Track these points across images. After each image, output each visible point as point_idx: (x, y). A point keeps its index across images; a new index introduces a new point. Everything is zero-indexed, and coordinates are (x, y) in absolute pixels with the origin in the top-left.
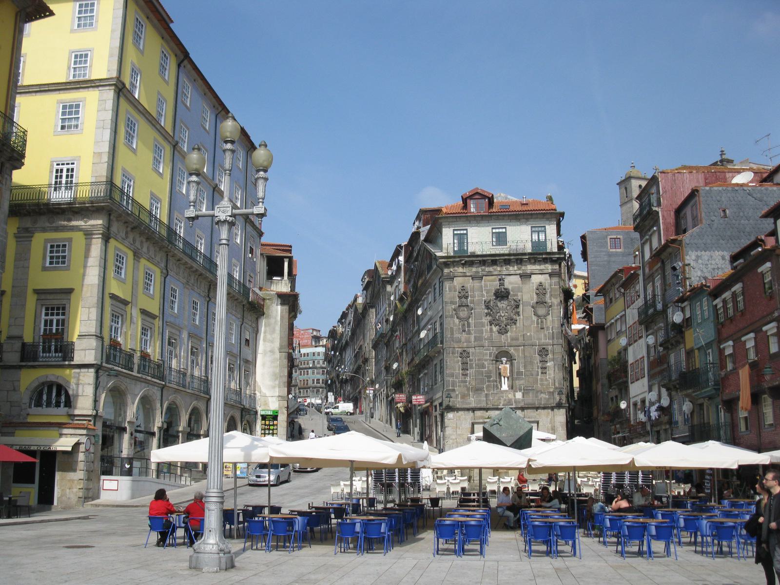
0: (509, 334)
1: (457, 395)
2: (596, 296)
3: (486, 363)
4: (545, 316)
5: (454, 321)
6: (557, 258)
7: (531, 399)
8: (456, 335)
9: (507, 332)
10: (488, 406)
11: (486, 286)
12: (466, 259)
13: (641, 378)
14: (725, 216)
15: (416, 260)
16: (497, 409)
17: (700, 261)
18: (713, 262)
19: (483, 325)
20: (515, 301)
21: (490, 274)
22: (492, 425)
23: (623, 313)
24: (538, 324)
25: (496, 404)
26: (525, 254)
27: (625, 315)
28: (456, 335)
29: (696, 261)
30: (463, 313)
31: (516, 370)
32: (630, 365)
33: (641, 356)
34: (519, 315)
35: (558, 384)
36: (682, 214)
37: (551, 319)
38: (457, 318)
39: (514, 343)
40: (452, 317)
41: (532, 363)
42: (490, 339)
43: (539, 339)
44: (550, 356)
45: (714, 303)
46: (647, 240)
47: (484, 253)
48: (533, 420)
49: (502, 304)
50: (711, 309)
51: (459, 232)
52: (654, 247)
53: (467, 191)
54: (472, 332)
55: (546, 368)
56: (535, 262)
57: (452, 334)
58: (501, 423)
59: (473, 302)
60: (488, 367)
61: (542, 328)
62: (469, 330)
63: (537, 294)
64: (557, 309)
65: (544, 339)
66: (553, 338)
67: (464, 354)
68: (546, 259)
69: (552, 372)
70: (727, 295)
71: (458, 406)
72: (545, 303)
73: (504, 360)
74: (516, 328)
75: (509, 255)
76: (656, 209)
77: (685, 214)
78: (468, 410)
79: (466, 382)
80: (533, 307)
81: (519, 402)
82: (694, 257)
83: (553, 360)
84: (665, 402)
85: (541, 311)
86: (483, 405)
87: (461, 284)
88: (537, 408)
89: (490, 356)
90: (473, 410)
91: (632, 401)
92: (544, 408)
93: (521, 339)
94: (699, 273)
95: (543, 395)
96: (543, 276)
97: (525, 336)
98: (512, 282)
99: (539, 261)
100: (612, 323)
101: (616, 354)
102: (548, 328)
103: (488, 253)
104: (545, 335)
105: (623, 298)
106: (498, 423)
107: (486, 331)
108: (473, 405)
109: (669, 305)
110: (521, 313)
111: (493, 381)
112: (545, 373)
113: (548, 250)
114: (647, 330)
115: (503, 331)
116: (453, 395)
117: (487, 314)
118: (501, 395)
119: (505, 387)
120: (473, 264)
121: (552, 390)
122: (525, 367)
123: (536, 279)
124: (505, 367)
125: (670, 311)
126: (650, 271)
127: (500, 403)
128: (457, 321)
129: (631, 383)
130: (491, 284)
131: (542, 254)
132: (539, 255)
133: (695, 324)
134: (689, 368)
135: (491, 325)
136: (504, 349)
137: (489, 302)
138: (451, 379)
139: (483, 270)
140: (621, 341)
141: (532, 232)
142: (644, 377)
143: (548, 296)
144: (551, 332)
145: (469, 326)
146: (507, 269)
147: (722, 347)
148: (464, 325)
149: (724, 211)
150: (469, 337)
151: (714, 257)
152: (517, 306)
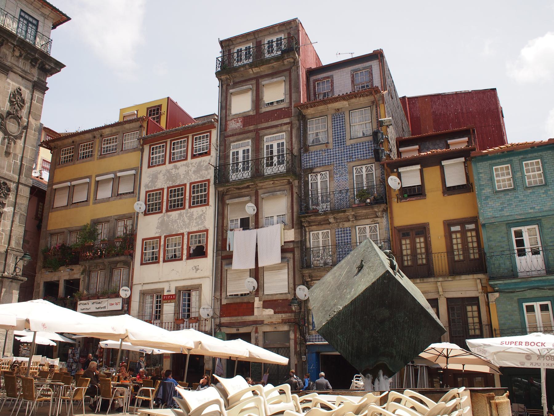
4: (16, 137)
6: (52, 68)
32: (143, 240)
33: (195, 229)
35: (16, 242)
37: (22, 145)
44: (11, 197)
63: (11, 102)
64: (34, 135)
69: (8, 223)
77: (332, 77)
83: (15, 205)
91: (137, 290)
96: (24, 80)
99: (26, 59)
104: (9, 166)
109: (315, 171)
129: (142, 264)
133: (487, 191)
141: (21, 16)
143: (25, 111)
144: (19, 164)
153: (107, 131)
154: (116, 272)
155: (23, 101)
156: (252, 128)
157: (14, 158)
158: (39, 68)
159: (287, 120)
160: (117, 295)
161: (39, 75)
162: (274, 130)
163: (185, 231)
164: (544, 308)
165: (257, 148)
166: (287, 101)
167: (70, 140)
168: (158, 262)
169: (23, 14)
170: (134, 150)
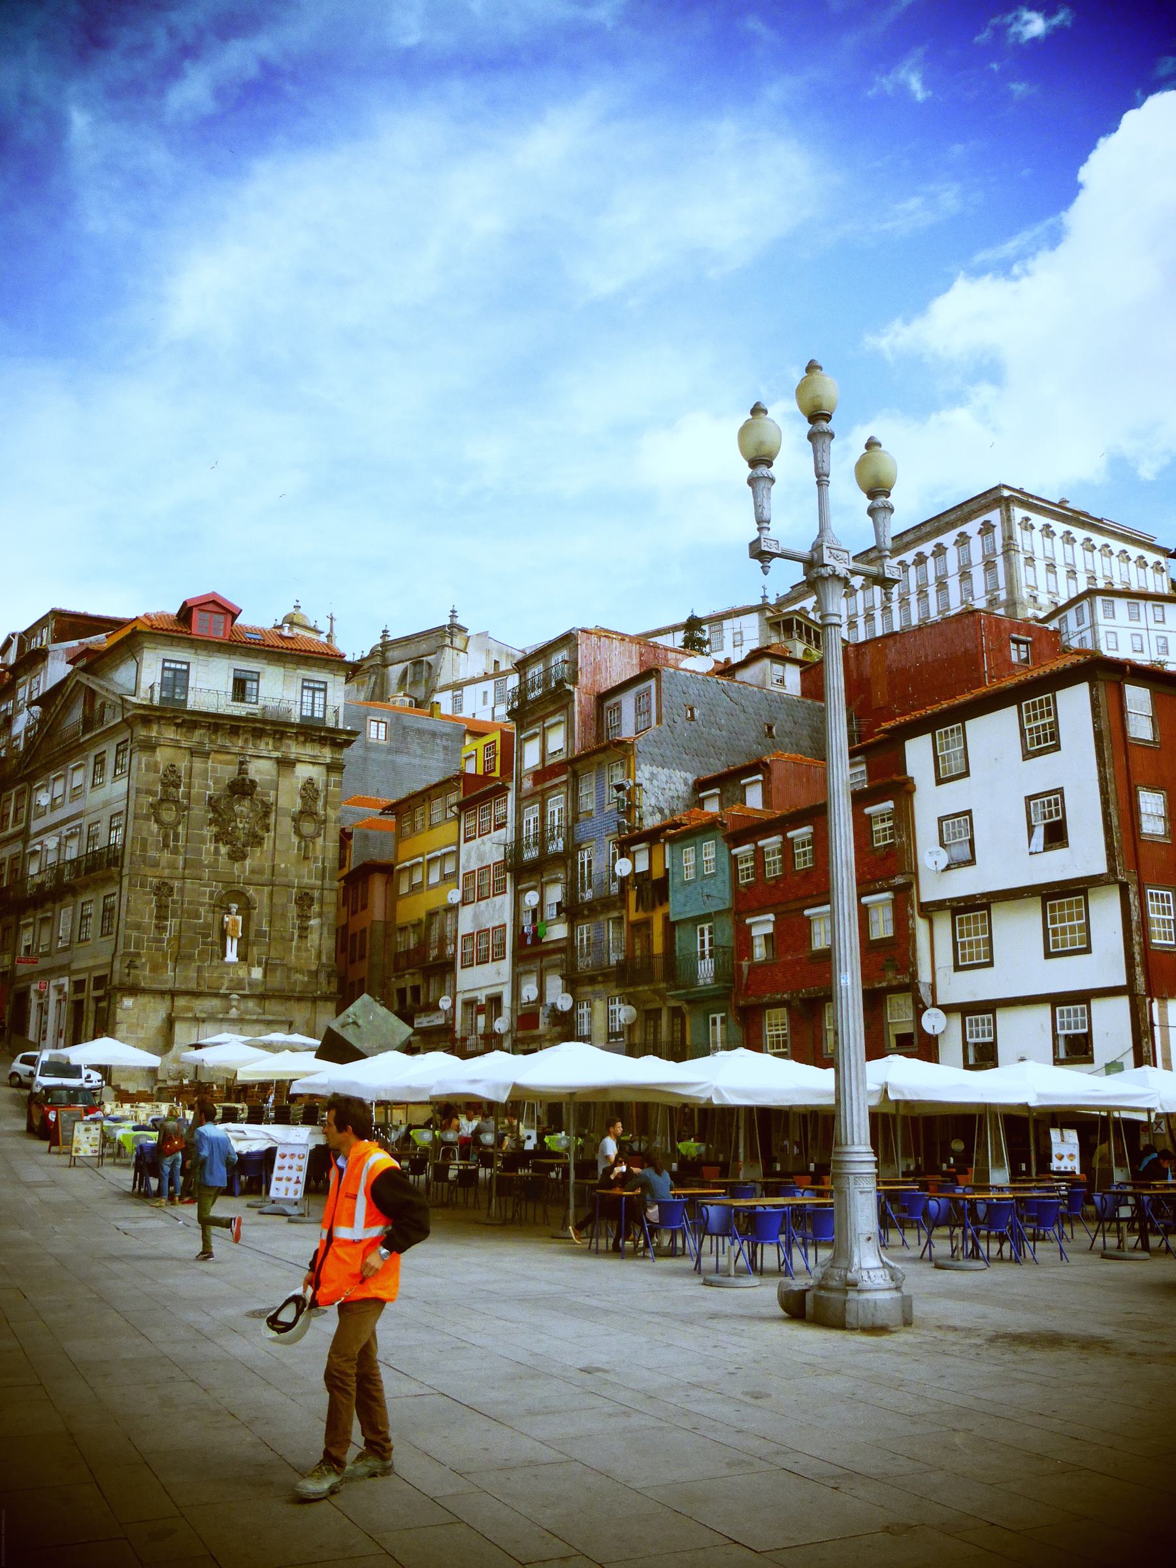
0: (248, 862)
1: (144, 964)
2: (381, 814)
3: (202, 910)
5: (149, 829)
7: (277, 980)
8: (152, 853)
9: (244, 857)
10: (201, 989)
11: (214, 770)
12: (186, 717)
13: (493, 960)
14: (692, 718)
15: (45, 700)
16: (217, 995)
17: (655, 782)
18: (673, 787)
19: (202, 840)
20: (263, 802)
21: (223, 750)
22: (343, 1026)
23: (454, 848)
24: (299, 849)
25: (215, 985)
26: (292, 725)
27: (457, 852)
28: (152, 853)
29: (651, 780)
30: (168, 816)
31: (253, 927)
33: (497, 924)
34: (268, 831)
36: (608, 704)
38: (157, 821)
39: (256, 878)
40: (147, 818)
41: (284, 916)
42: (213, 866)
43: (300, 877)
44: (316, 908)
45: (734, 851)
46: (535, 735)
47: (221, 711)
48: (283, 1018)
49: (243, 807)
50: (725, 860)
51: (173, 665)
52: (551, 748)
53: (195, 591)
54: (182, 850)
55: (306, 928)
56: (305, 741)
57: (144, 848)
58: (360, 1022)
59: (188, 796)
60: (206, 917)
61: (306, 858)
62: (176, 847)
63: (302, 797)
65: (306, 876)
66: (323, 878)
67: (163, 890)
68: (325, 738)
70: (772, 842)
71: (143, 984)
72: (316, 814)
73: (234, 907)
74: (262, 852)
75: (264, 721)
76: (569, 687)
78: (162, 993)
79: (161, 941)
80: (294, 819)
81: (257, 985)
82: (647, 775)
83: (320, 915)
84: (564, 1002)
85: (308, 828)
86: (193, 986)
87: (168, 760)
88: (289, 998)
89: (211, 898)
90: (173, 994)
92: (300, 999)
93: (268, 871)
94: (653, 802)
95: (299, 976)
97: (276, 868)
98: (260, 770)
99: (313, 741)
100: (419, 864)
101: (423, 916)
102: (316, 859)
103: (228, 712)
104: (310, 872)
105: (456, 822)
106: (355, 1023)
107: (208, 851)
108: (168, 986)
109: (583, 846)
110: (272, 827)
111: (213, 944)
112: (306, 937)
113: (331, 724)
114: (517, 881)
115: (237, 856)
116: (138, 963)
117: (211, 822)
118: (225, 970)
119: (232, 956)
120: (196, 728)
121: (314, 968)
122: (270, 922)
123: (304, 771)
124: (233, 920)
125: (584, 857)
126: (535, 784)
127: (222, 984)
128: (155, 827)
129: (462, 967)
130: (227, 771)
131: (320, 729)
132: (312, 731)
134: (634, 951)
135: (217, 841)
136: (236, 887)
137: (219, 799)
138: (134, 934)
139: (211, 742)
140: (450, 895)
141: (304, 687)
142: (504, 958)
143: (320, 803)
145: (176, 837)
146: (255, 747)
147: (748, 921)
148: (166, 837)
149: (691, 709)
150: (175, 860)
151: (674, 779)
152: (266, 815)
153: (432, 792)
154: (448, 977)
155: (317, 791)
156: (539, 788)
157: (315, 862)
158: (331, 745)
159: (564, 778)
160: (438, 1009)
161: (333, 752)
162: (555, 792)
163: (490, 925)
164: (723, 1020)
165: (543, 817)
166: (565, 750)
167: (406, 805)
168: (472, 965)
169: (306, 684)
170: (451, 819)
